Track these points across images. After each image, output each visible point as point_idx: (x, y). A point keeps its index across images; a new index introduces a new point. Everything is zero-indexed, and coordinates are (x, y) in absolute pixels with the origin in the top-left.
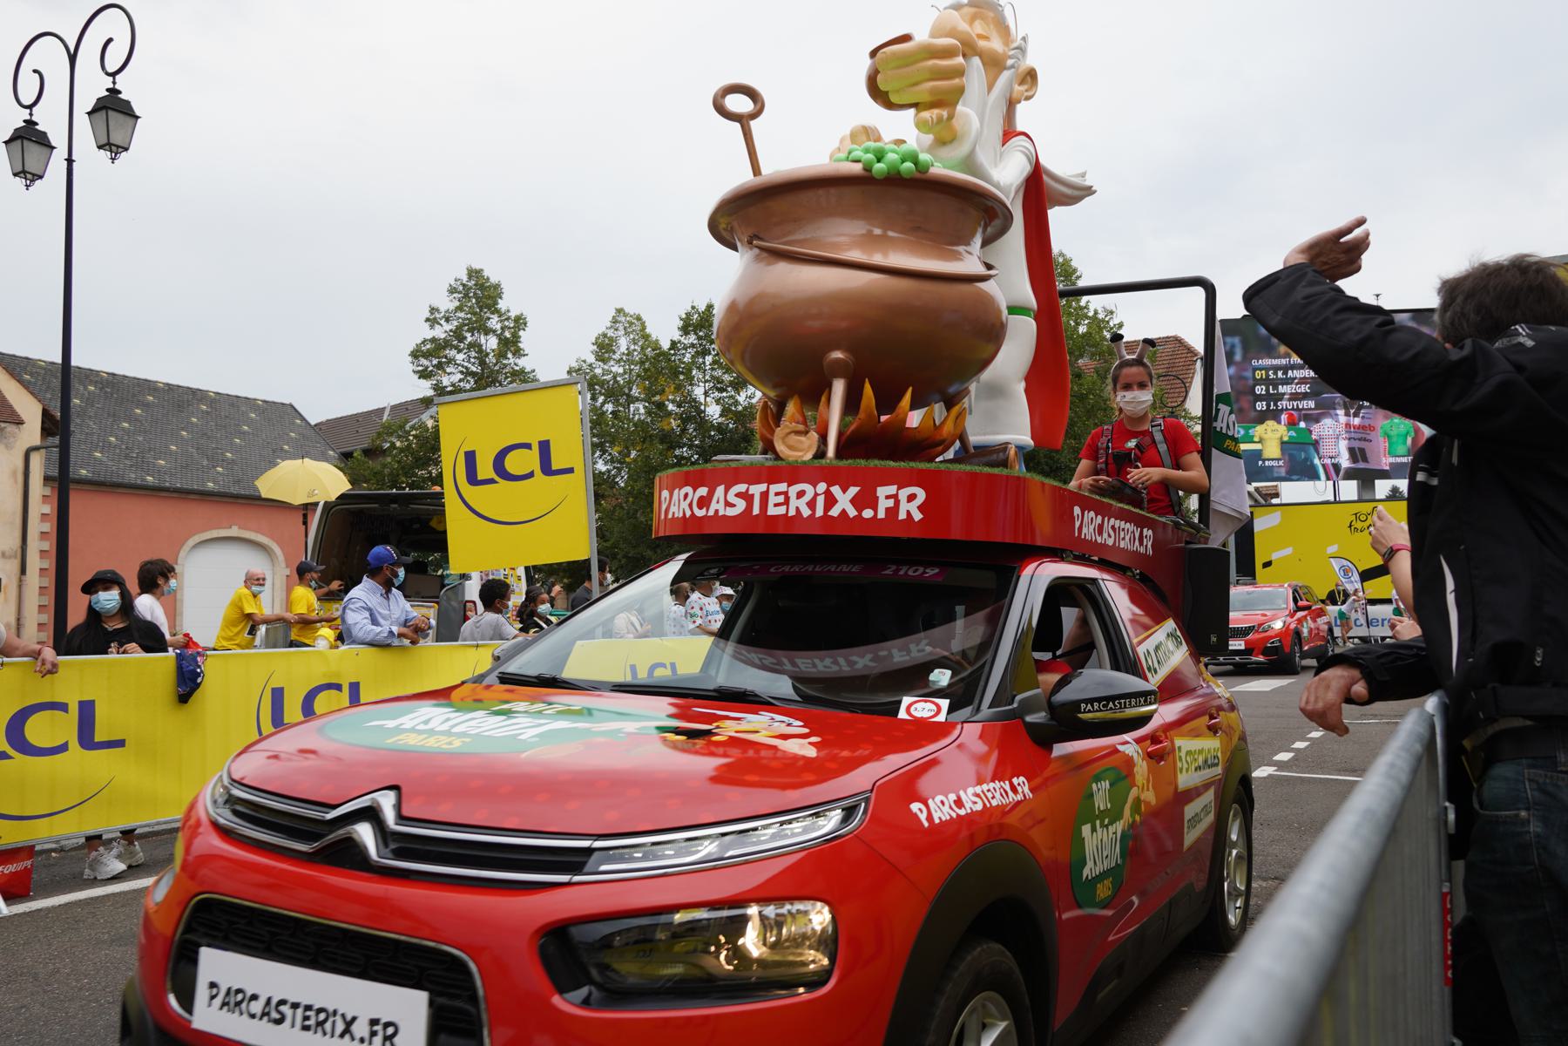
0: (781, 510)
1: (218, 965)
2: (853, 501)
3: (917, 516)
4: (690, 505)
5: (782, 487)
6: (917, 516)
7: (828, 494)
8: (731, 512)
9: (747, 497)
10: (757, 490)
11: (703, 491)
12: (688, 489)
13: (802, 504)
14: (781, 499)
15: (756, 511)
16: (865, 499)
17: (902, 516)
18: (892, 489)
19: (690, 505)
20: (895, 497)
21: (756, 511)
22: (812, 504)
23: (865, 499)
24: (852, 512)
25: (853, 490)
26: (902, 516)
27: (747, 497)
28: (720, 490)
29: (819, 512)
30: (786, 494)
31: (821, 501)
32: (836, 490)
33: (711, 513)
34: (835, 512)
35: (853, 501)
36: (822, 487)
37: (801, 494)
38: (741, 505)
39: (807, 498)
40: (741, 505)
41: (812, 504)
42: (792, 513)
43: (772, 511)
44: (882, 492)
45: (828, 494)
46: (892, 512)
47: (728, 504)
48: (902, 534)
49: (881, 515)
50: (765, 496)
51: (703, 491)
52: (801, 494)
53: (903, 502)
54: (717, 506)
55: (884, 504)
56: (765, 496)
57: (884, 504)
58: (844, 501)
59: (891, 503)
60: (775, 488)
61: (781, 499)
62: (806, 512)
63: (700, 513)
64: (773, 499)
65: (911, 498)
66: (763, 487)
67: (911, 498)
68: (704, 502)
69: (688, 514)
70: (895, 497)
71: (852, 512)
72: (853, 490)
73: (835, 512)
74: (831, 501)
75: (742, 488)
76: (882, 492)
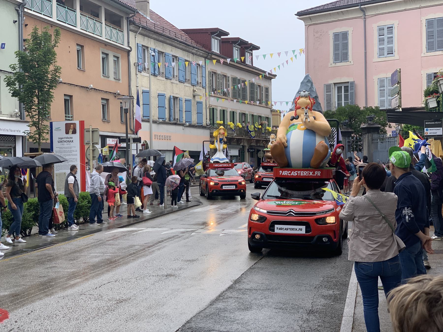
1: (276, 226)
10: (299, 172)
11: (290, 172)
23: (313, 174)
27: (298, 173)
28: (293, 172)
38: (296, 174)
44: (316, 172)
46: (317, 175)
48: (318, 178)
50: (300, 173)
51: (290, 172)
53: (318, 173)
54: (292, 174)
55: (316, 174)
56: (300, 173)
57: (316, 174)
58: (311, 173)
68: (289, 173)
74: (309, 173)
76: (316, 172)
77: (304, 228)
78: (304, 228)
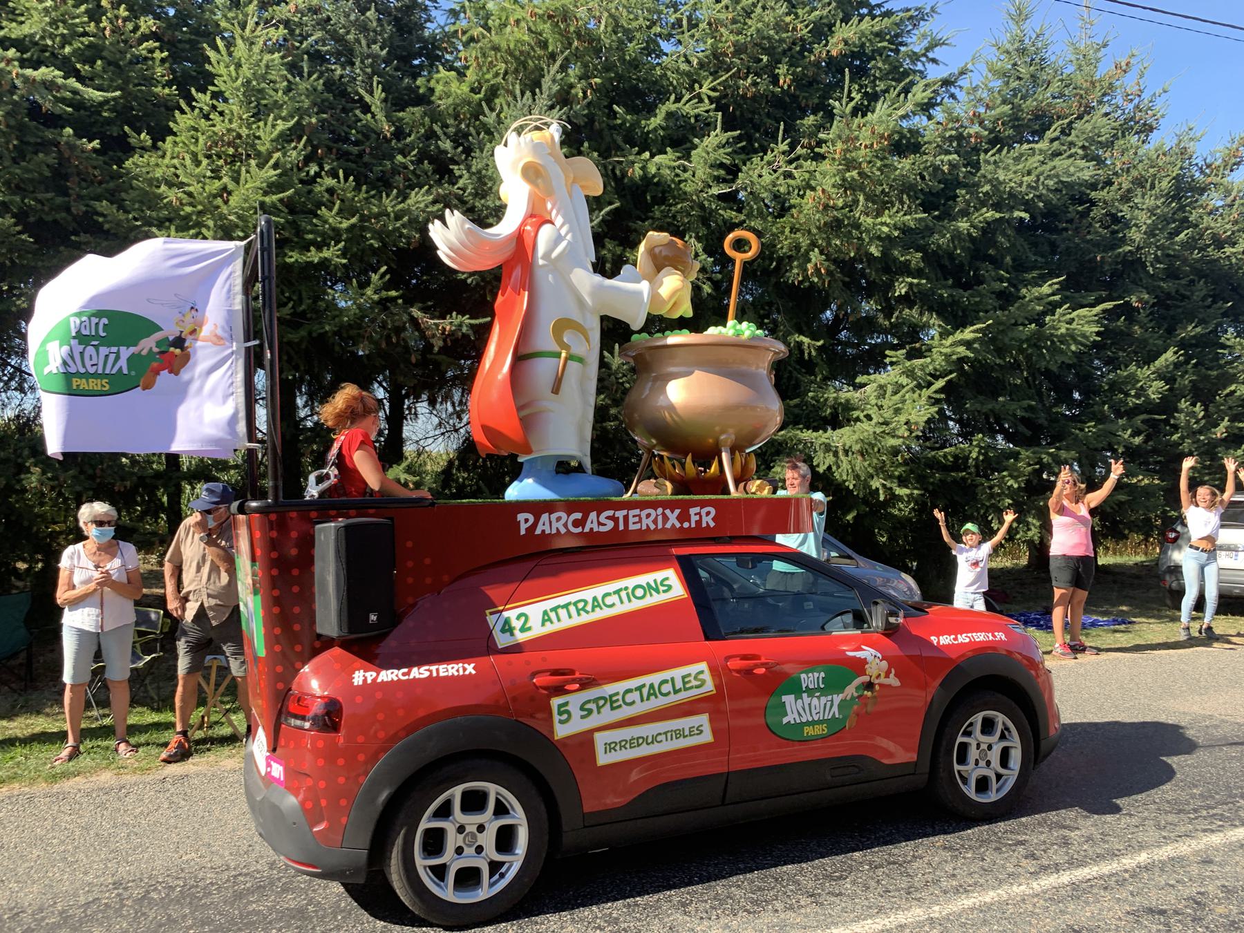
0: (637, 527)
2: (678, 518)
3: (712, 524)
4: (565, 525)
5: (637, 512)
6: (712, 524)
7: (664, 514)
8: (602, 529)
9: (614, 519)
10: (620, 514)
11: (578, 516)
12: (563, 515)
13: (650, 521)
14: (637, 519)
15: (621, 527)
16: (684, 517)
17: (704, 525)
18: (697, 509)
19: (565, 525)
20: (699, 514)
21: (621, 527)
22: (655, 522)
23: (684, 517)
24: (678, 525)
25: (677, 512)
26: (704, 525)
27: (614, 519)
28: (593, 515)
29: (660, 526)
30: (639, 516)
31: (660, 518)
32: (668, 512)
33: (587, 530)
34: (668, 525)
35: (678, 518)
36: (660, 510)
37: (648, 516)
38: (610, 524)
39: (652, 517)
40: (610, 524)
41: (655, 522)
42: (644, 527)
43: (632, 527)
44: (693, 511)
45: (664, 514)
46: (699, 523)
47: (600, 524)
49: (693, 525)
50: (626, 518)
51: (578, 516)
52: (648, 516)
54: (592, 524)
55: (694, 518)
56: (626, 518)
57: (694, 518)
58: (673, 517)
59: (697, 518)
60: (632, 513)
61: (637, 519)
62: (652, 527)
63: (579, 530)
64: (631, 520)
65: (708, 514)
66: (625, 512)
67: (708, 514)
68: (576, 523)
69: (563, 531)
70: (699, 514)
71: (678, 525)
72: (677, 512)
73: (668, 525)
75: (610, 513)
76: (693, 511)
77: (703, 720)
78: (703, 720)
